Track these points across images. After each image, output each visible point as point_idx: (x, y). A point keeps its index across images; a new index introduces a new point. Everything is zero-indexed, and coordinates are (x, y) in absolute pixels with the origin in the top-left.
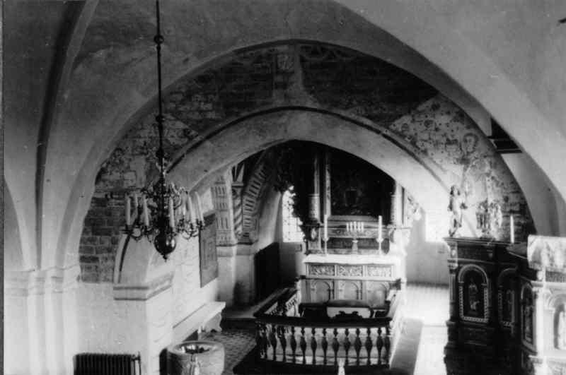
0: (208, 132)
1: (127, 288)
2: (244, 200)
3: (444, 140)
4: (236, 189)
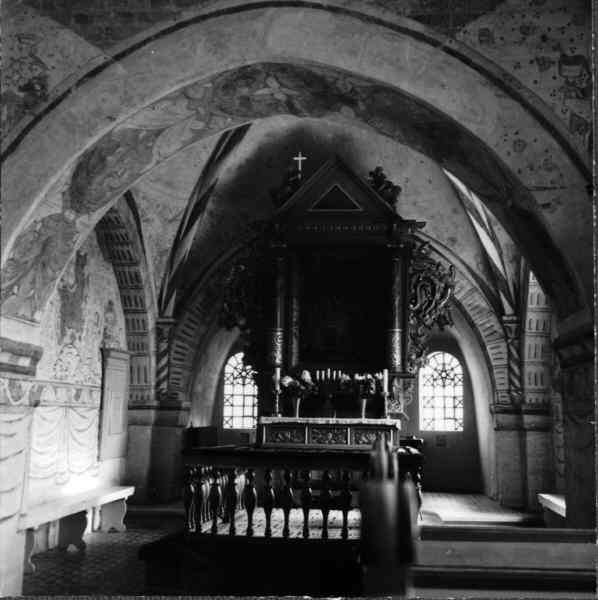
0: (120, 47)
3: (556, 56)
4: (161, 327)
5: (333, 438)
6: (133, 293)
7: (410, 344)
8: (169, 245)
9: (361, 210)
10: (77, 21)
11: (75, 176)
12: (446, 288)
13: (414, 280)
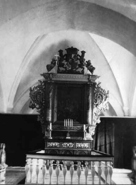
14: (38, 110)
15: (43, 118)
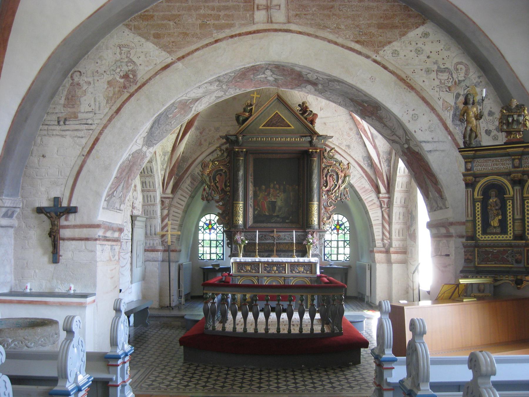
0: (180, 54)
1: (75, 227)
2: (171, 212)
3: (435, 67)
4: (163, 199)
5: (277, 270)
6: (147, 180)
7: (323, 211)
8: (170, 149)
9: (293, 127)
10: (154, 38)
11: (152, 127)
12: (345, 177)
13: (326, 171)
14: (217, 204)
15: (227, 218)
